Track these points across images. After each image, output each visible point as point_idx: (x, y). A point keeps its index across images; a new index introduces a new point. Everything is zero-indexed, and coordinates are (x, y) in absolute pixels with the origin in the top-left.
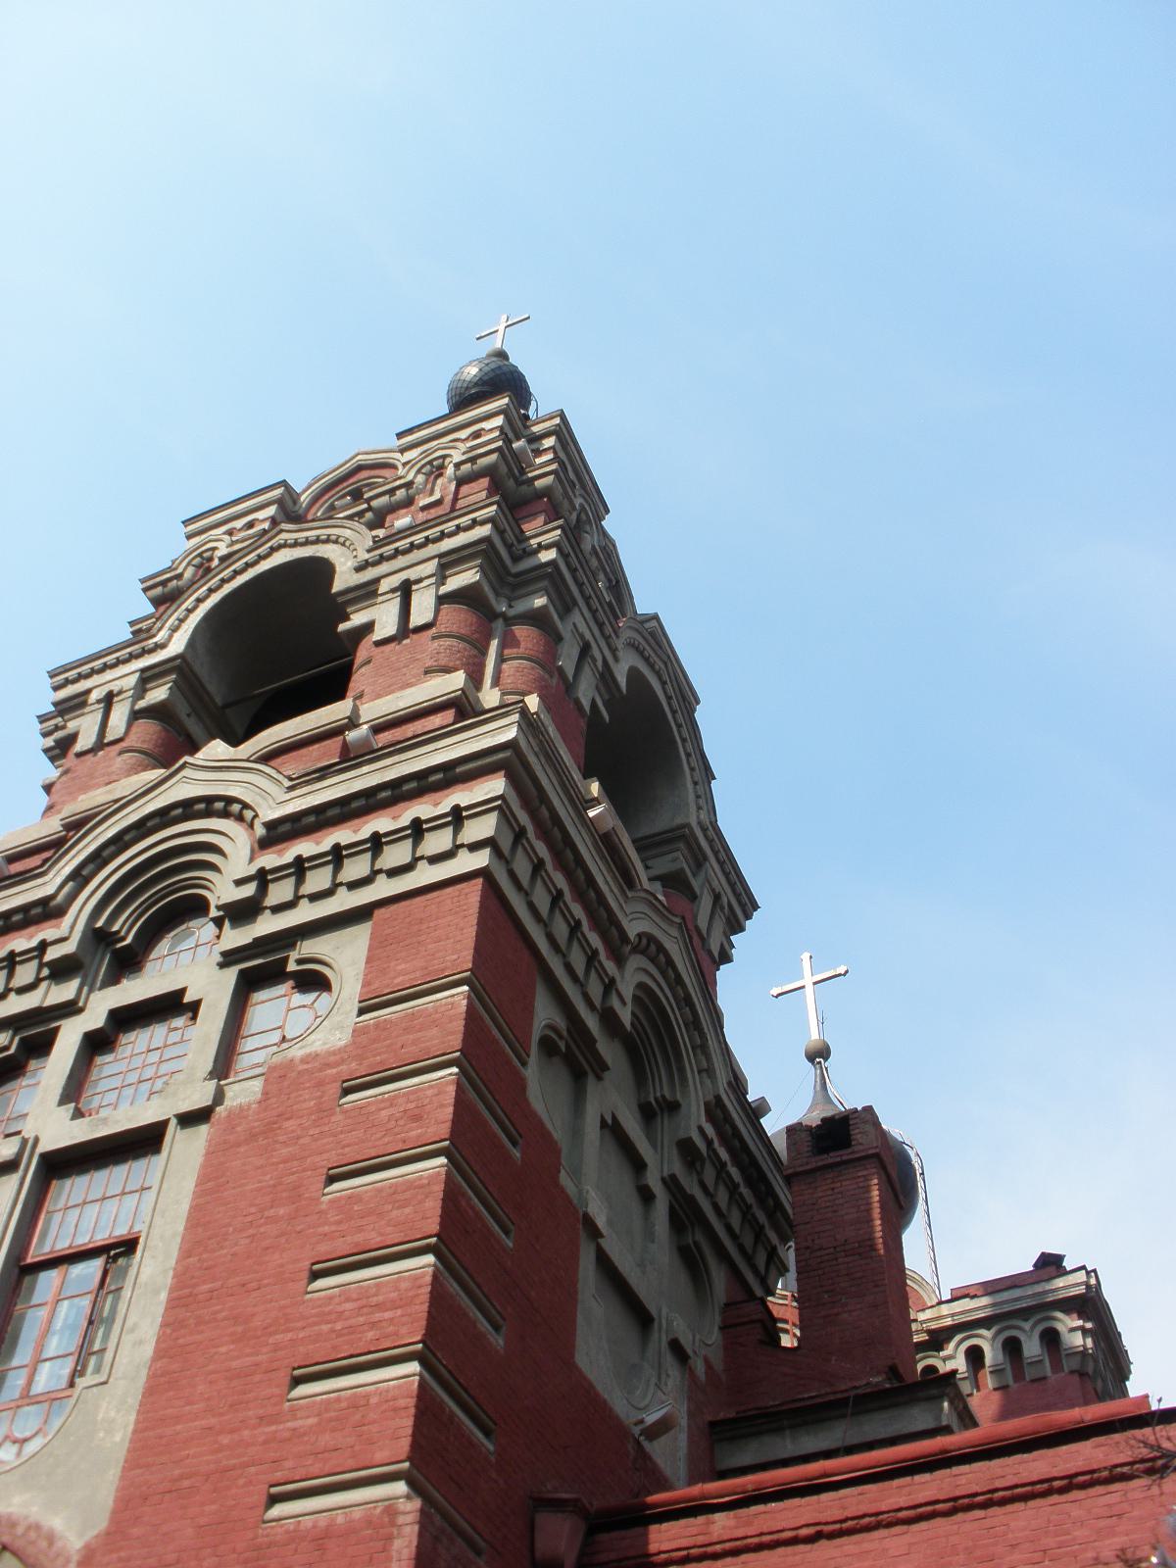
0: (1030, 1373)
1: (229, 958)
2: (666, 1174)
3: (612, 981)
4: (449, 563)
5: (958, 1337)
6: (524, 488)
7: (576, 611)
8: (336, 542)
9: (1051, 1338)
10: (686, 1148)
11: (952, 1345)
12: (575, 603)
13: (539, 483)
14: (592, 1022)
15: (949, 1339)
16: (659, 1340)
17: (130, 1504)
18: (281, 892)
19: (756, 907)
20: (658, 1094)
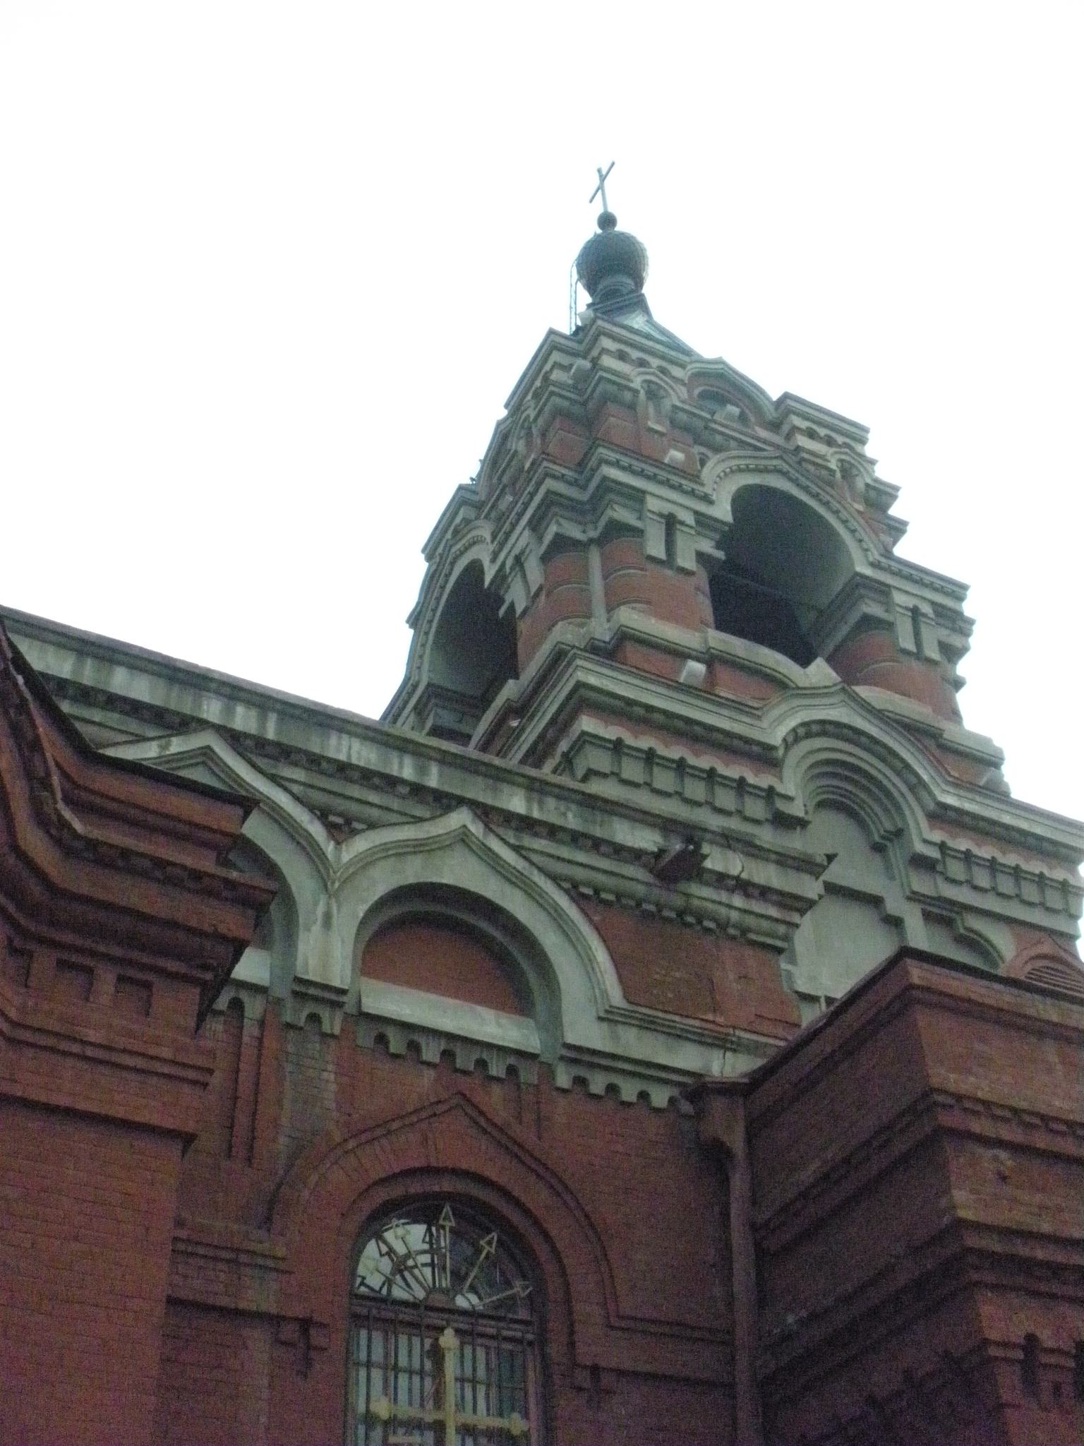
7: (649, 499)
8: (474, 543)
12: (644, 492)
19: (964, 587)
20: (882, 832)
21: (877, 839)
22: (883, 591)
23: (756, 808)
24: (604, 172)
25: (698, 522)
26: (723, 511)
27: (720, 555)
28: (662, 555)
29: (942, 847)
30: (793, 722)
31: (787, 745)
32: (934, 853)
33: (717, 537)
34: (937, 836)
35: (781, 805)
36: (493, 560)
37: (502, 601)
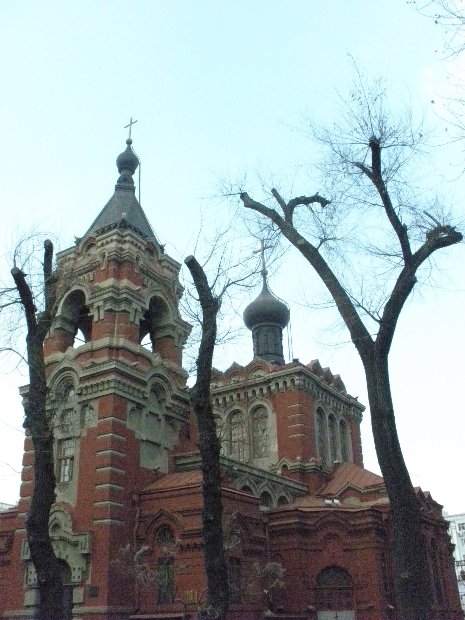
0: (289, 389)
1: (79, 403)
2: (163, 413)
4: (105, 301)
5: (274, 381)
6: (122, 259)
9: (293, 381)
10: (167, 408)
11: (272, 383)
12: (132, 301)
13: (126, 258)
14: (141, 402)
16: (162, 447)
17: (79, 501)
18: (84, 392)
22: (174, 328)
23: (141, 396)
24: (133, 121)
26: (147, 307)
27: (144, 319)
29: (173, 404)
30: (151, 374)
31: (149, 379)
34: (172, 401)
35: (146, 395)
36: (90, 299)
37: (89, 312)
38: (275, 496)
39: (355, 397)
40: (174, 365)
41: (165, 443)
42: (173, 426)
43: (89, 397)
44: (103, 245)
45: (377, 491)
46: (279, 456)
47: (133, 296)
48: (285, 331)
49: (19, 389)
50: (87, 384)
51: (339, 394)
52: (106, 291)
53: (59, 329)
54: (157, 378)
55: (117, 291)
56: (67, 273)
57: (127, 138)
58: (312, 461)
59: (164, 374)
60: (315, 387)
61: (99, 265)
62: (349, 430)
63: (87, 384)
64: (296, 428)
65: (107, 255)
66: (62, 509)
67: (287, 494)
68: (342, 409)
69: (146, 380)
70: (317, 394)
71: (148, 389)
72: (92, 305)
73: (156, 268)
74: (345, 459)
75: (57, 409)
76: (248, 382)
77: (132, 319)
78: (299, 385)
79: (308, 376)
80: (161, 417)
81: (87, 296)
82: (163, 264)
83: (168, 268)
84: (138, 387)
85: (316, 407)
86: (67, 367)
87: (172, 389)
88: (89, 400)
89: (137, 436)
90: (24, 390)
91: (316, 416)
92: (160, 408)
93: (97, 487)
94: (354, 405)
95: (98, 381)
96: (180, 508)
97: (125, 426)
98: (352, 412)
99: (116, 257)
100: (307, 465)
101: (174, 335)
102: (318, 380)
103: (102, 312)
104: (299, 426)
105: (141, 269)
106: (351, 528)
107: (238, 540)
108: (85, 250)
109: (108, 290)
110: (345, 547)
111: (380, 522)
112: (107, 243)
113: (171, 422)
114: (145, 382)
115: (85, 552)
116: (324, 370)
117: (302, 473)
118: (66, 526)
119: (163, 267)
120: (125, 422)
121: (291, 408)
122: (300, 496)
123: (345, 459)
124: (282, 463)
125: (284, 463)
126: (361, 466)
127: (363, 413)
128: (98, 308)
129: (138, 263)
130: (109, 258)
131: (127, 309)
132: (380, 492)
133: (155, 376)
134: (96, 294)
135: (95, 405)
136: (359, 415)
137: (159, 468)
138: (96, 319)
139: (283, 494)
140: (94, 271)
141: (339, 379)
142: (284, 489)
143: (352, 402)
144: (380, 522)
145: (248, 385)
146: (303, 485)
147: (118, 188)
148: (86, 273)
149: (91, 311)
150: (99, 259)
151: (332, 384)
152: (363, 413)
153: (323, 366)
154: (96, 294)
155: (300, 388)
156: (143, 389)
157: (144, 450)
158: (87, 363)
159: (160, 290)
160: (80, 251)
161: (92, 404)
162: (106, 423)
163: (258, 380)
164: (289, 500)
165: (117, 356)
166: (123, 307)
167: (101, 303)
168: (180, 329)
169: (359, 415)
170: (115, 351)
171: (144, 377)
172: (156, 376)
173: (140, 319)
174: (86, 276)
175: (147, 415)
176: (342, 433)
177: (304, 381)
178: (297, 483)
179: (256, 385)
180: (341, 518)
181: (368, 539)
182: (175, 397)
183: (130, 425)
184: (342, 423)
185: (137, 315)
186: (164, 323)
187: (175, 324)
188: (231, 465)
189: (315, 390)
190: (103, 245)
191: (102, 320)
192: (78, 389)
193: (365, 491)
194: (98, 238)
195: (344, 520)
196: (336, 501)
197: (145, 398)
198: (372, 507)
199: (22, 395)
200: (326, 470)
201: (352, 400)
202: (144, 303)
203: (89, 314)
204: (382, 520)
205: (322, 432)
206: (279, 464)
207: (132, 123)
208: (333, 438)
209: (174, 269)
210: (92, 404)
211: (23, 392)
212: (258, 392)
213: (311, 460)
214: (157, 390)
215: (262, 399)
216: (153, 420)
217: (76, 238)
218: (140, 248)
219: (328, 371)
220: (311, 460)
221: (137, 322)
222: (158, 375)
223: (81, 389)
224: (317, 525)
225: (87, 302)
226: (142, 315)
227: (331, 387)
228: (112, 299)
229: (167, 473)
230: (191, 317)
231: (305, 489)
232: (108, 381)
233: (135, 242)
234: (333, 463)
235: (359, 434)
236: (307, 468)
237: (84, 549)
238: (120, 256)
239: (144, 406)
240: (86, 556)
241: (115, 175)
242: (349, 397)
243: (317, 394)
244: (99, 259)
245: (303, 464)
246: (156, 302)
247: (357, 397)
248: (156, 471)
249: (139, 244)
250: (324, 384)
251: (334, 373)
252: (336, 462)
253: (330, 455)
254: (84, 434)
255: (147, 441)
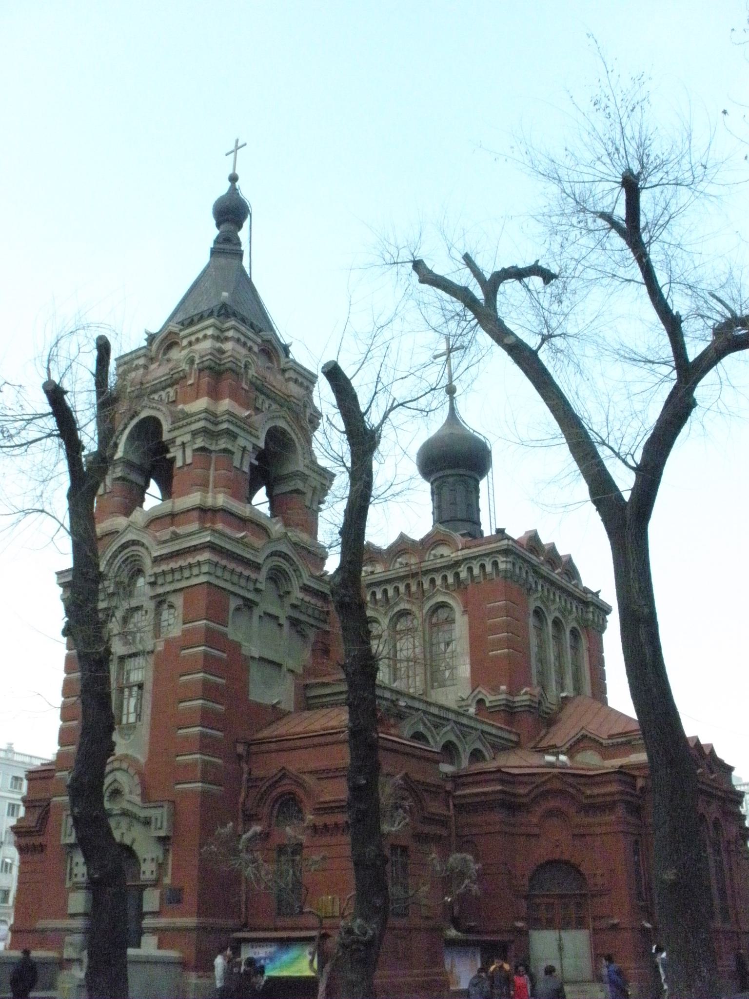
0: (488, 578)
1: (153, 598)
3: (256, 580)
4: (195, 434)
5: (464, 563)
9: (495, 564)
10: (294, 606)
11: (462, 566)
13: (227, 365)
14: (249, 596)
15: (462, 563)
16: (284, 669)
18: (160, 581)
21: (282, 593)
22: (304, 477)
24: (239, 145)
25: (253, 448)
26: (262, 444)
27: (256, 463)
28: (238, 466)
30: (268, 552)
32: (298, 603)
33: (257, 453)
34: (301, 595)
35: (259, 586)
36: (169, 432)
38: (464, 750)
39: (594, 591)
40: (304, 537)
41: (289, 663)
42: (302, 635)
43: (168, 588)
44: (190, 344)
45: (628, 743)
46: (472, 683)
47: (238, 426)
48: (483, 484)
49: (56, 576)
50: (165, 567)
51: (570, 587)
52: (196, 417)
53: (118, 479)
54: (276, 558)
55: (212, 419)
56: (133, 389)
57: (230, 172)
58: (526, 693)
59: (289, 553)
60: (531, 573)
61: (184, 377)
62: (584, 643)
63: (165, 567)
64: (500, 640)
65: (197, 361)
66: (125, 766)
67: (484, 745)
68: (574, 609)
69: (260, 561)
70: (534, 586)
71: (262, 576)
72: (173, 441)
73: (276, 381)
74: (578, 690)
75: (116, 608)
76: (423, 565)
77: (237, 463)
78: (506, 571)
79: (519, 556)
80: (283, 621)
81: (166, 426)
82: (287, 375)
83: (296, 381)
84: (247, 573)
85: (532, 608)
86: (134, 541)
87: (301, 576)
88: (168, 592)
89: (244, 651)
90: (64, 577)
91: (532, 621)
92: (282, 607)
93: (180, 731)
94: (593, 604)
95: (182, 562)
96: (312, 766)
97: (225, 635)
98: (590, 616)
99: (213, 364)
100: (517, 699)
101: (305, 490)
102: (536, 564)
103: (189, 452)
104: (503, 638)
105: (252, 383)
106: (585, 801)
107: (404, 818)
108: (162, 351)
109: (199, 416)
110: (576, 831)
111: (633, 792)
112: (198, 340)
113: (299, 629)
114: (259, 564)
115: (162, 833)
116: (546, 548)
117: (510, 712)
118: (131, 793)
119: (288, 380)
120: (225, 629)
121: (493, 607)
122: (505, 749)
123: (578, 690)
124: (475, 697)
125: (480, 696)
126: (604, 701)
127: (608, 617)
128: (183, 444)
129: (247, 372)
130: (201, 366)
131: (229, 447)
132: (633, 743)
133: (273, 554)
134: (180, 424)
135: (178, 601)
136: (601, 619)
137: (278, 703)
138: (179, 463)
139: (478, 745)
140: (175, 387)
141: (569, 561)
142: (479, 738)
143: (590, 600)
144: (633, 792)
145: (424, 569)
146: (510, 732)
147: (214, 252)
148: (164, 389)
149: (171, 450)
150: (185, 366)
151: (559, 570)
152: (608, 617)
153: (545, 540)
154: (180, 424)
155: (508, 576)
156: (253, 576)
157: (255, 673)
158: (166, 534)
159: (284, 417)
160: (153, 354)
161: (172, 599)
162: (194, 630)
163: (439, 562)
164: (486, 754)
165: (213, 523)
166: (223, 444)
167: (187, 438)
168: (315, 480)
169: (601, 619)
170: (209, 513)
171: (256, 556)
172: (275, 555)
173: (251, 465)
174: (163, 394)
175: (260, 616)
176: (575, 648)
177: (514, 564)
178: (501, 728)
179: (436, 570)
180: (571, 785)
181: (613, 817)
182: (305, 589)
183: (234, 632)
184: (574, 632)
185: (246, 457)
186: (291, 468)
187: (307, 472)
188: (394, 699)
189: (531, 579)
190: (190, 344)
191: (189, 465)
192: (150, 576)
193: (610, 741)
194: (182, 334)
195: (574, 787)
196: (563, 758)
197: (257, 591)
198: (621, 767)
199: (61, 585)
200: (547, 707)
201: (590, 595)
202: (257, 437)
203: (169, 456)
204: (635, 790)
205: (541, 646)
206: (471, 698)
207: (237, 148)
208: (559, 657)
209: (306, 383)
210: (172, 599)
211: (63, 581)
212: (439, 582)
213: (523, 691)
214: (277, 577)
215: (445, 593)
216: (271, 625)
217: (147, 333)
218: (250, 349)
219: (553, 548)
220: (523, 691)
221: (246, 469)
222: (278, 553)
223: (156, 575)
224: (532, 795)
225: (166, 436)
226: (254, 456)
227: (556, 575)
228: (205, 431)
229: (292, 710)
230: (332, 459)
231: (514, 738)
232: (198, 562)
233: (243, 339)
234: (557, 696)
235: (601, 650)
236: (517, 704)
237: (160, 829)
238: (218, 362)
239: (256, 604)
240: (163, 841)
241: (211, 232)
242: (586, 591)
243: (534, 586)
244: (185, 366)
245: (511, 698)
246: (276, 436)
247: (599, 591)
248: (274, 706)
249: (250, 343)
250: (545, 569)
251: (562, 551)
252: (564, 695)
253: (554, 683)
254: (160, 648)
255: (261, 659)
